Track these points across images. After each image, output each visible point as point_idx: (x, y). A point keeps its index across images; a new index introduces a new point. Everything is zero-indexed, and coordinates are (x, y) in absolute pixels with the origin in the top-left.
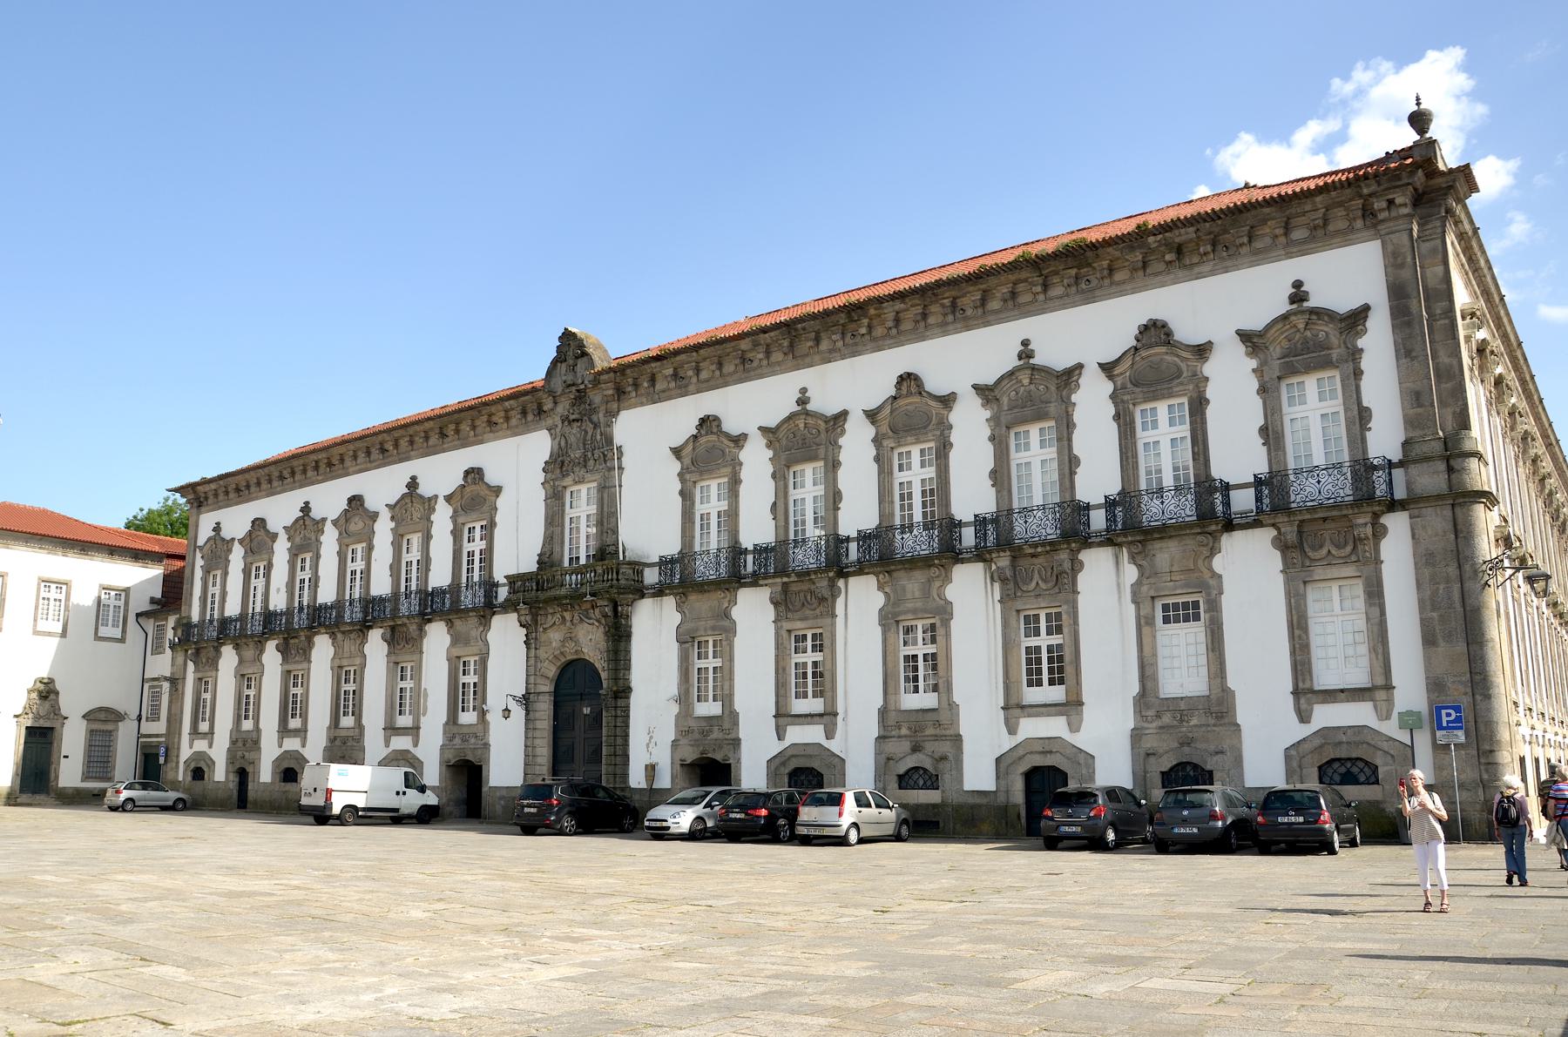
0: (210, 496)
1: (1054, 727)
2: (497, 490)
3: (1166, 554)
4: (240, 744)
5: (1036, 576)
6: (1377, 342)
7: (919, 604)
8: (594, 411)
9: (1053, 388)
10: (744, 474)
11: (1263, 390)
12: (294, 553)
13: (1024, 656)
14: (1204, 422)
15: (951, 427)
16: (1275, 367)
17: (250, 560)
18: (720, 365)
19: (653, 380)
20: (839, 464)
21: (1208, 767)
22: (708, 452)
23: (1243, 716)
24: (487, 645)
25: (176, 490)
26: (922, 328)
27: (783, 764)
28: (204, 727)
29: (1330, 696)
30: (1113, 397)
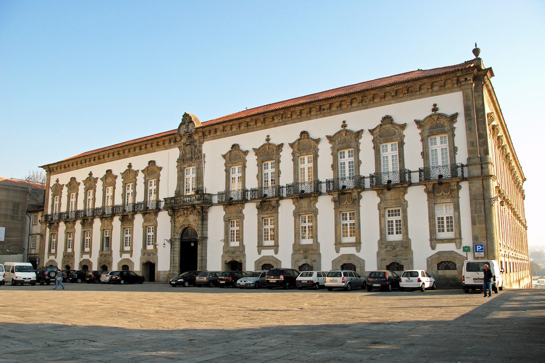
0: (55, 169)
1: (351, 250)
2: (161, 169)
3: (389, 195)
4: (67, 257)
5: (346, 200)
6: (460, 125)
7: (307, 209)
8: (195, 141)
9: (353, 137)
11: (422, 140)
12: (86, 190)
13: (342, 227)
14: (403, 150)
15: (318, 150)
16: (426, 133)
17: (70, 192)
18: (239, 127)
19: (216, 131)
20: (280, 161)
21: (402, 264)
22: (235, 157)
23: (413, 247)
24: (157, 222)
25: (42, 167)
26: (309, 116)
27: (260, 263)
28: (53, 251)
29: (442, 241)
30: (373, 141)
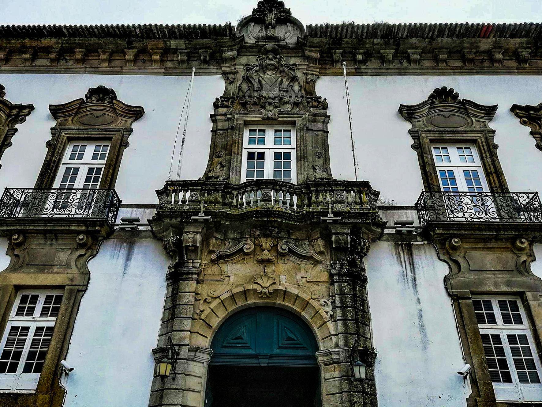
2: (137, 113)
24: (87, 275)
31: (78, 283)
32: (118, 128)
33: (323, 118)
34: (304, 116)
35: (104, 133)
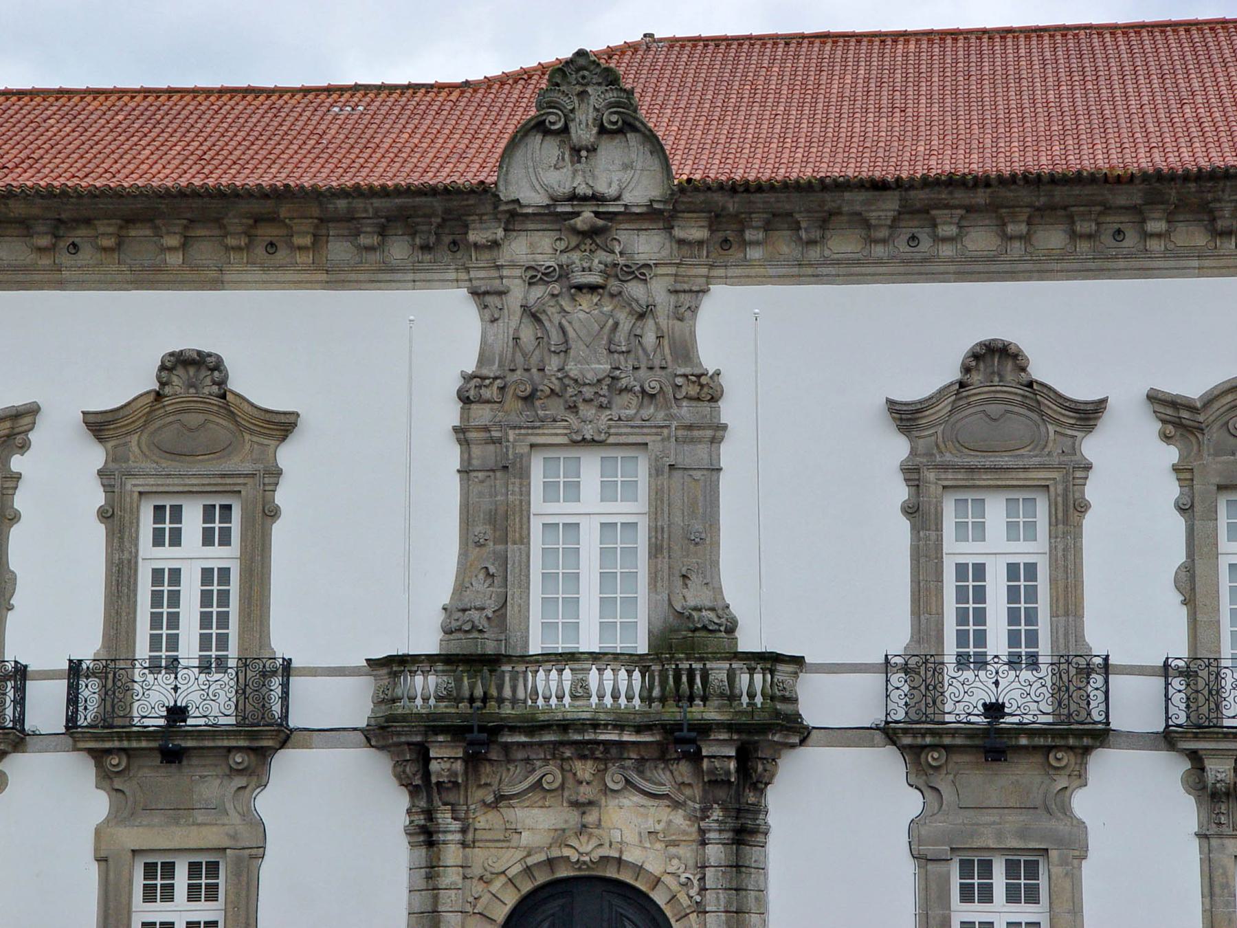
2: (282, 426)
8: (639, 272)
10: (1092, 492)
22: (991, 431)
24: (259, 826)
31: (247, 844)
32: (247, 467)
33: (709, 433)
34: (666, 431)
35: (219, 481)
